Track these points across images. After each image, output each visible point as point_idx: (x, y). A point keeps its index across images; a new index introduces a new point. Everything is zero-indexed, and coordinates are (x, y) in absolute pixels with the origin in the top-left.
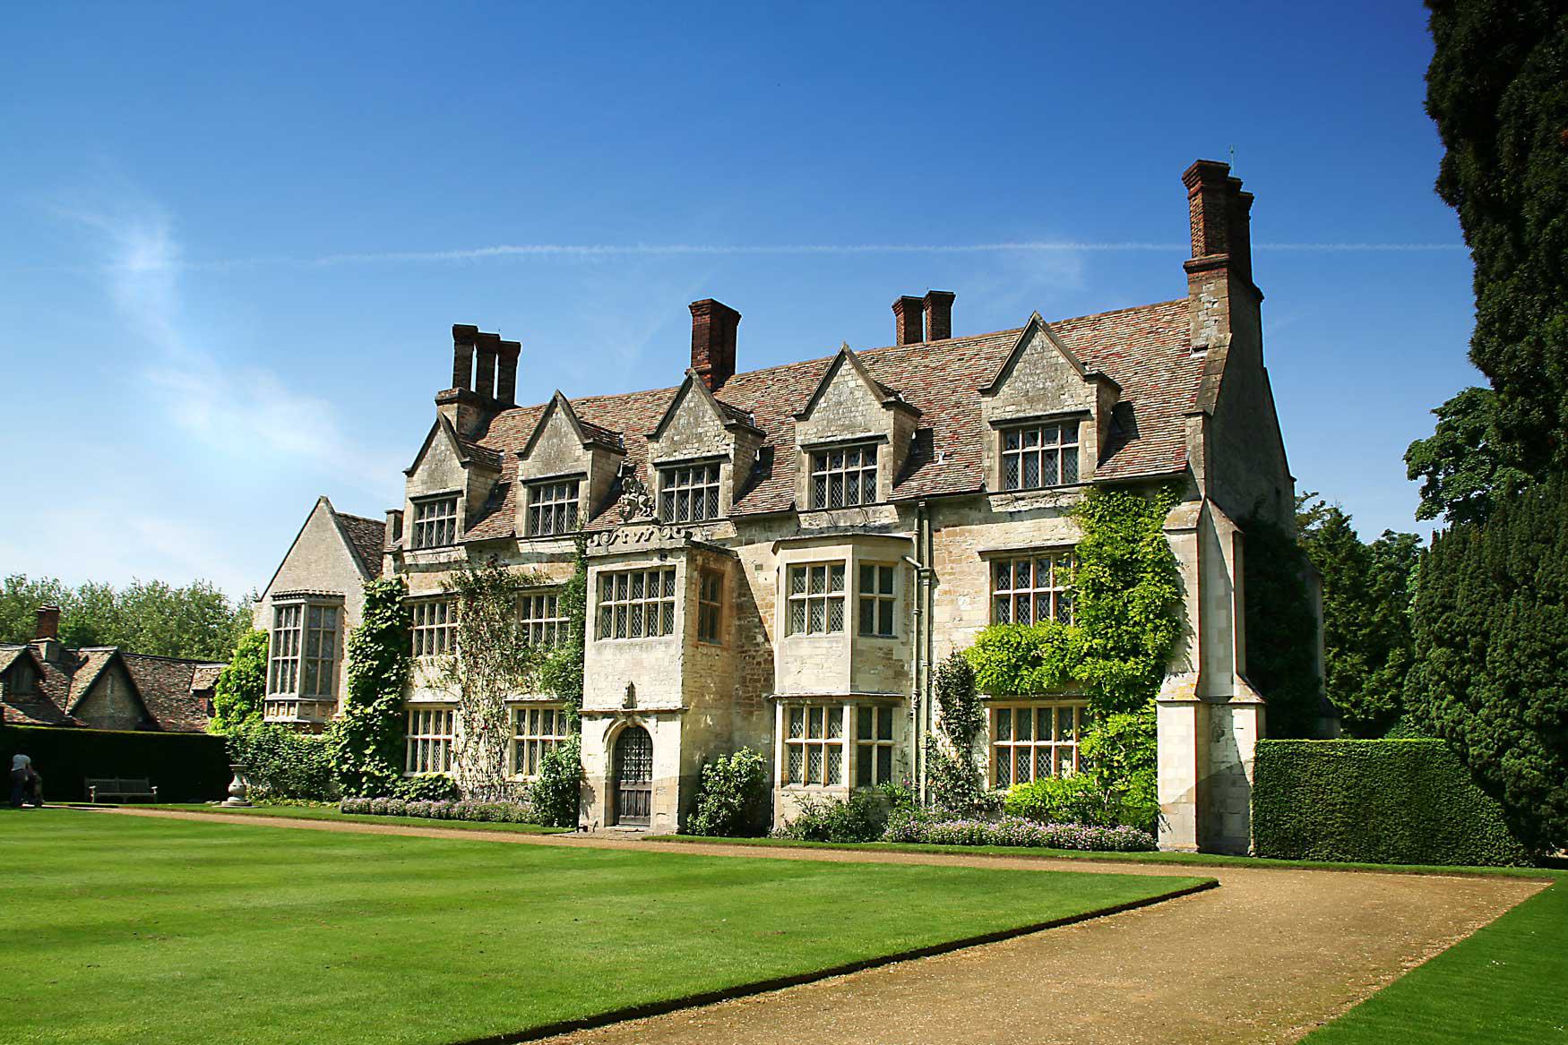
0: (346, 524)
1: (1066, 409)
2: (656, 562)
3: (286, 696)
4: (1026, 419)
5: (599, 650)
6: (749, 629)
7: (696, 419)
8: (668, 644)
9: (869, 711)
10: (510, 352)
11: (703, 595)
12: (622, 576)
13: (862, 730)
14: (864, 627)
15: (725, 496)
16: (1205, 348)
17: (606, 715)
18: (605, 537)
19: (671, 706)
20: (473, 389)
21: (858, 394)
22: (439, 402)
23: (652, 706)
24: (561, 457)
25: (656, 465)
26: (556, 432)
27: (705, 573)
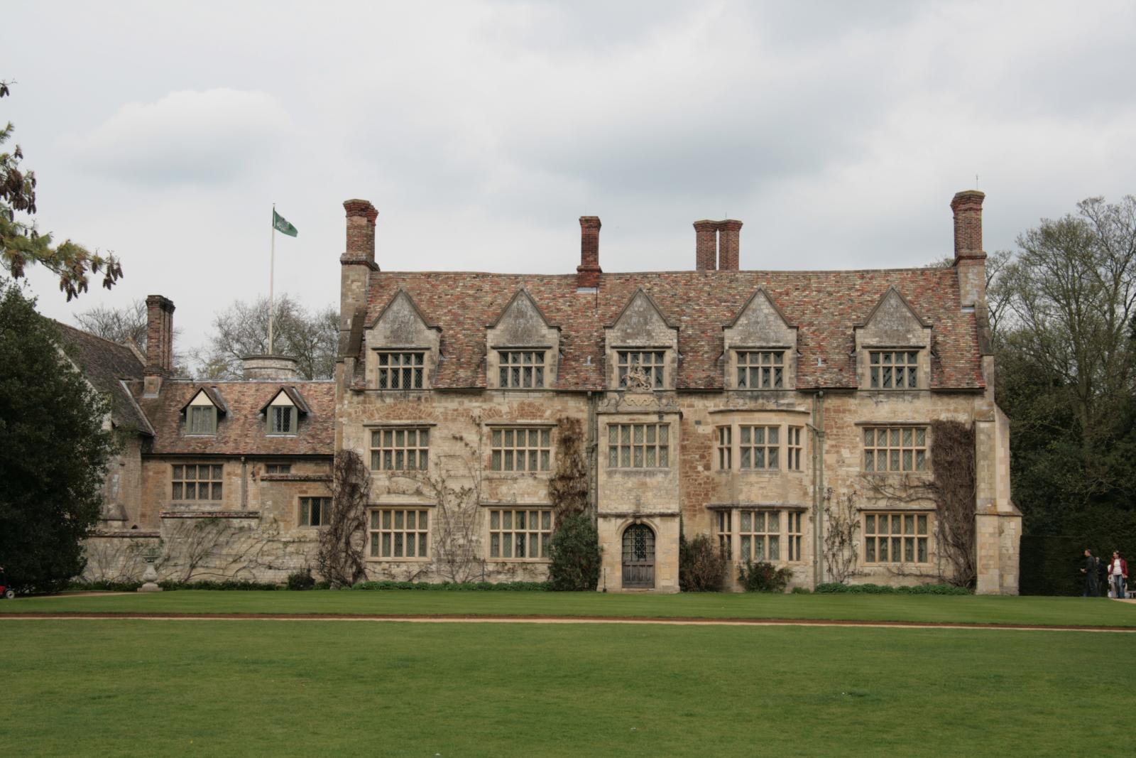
1: (911, 344)
2: (654, 418)
4: (886, 347)
5: (610, 474)
6: (692, 462)
7: (645, 320)
8: (666, 473)
12: (625, 427)
15: (670, 374)
16: (973, 306)
17: (619, 516)
19: (670, 511)
22: (344, 263)
23: (657, 511)
24: (527, 332)
25: (613, 347)
26: (521, 314)
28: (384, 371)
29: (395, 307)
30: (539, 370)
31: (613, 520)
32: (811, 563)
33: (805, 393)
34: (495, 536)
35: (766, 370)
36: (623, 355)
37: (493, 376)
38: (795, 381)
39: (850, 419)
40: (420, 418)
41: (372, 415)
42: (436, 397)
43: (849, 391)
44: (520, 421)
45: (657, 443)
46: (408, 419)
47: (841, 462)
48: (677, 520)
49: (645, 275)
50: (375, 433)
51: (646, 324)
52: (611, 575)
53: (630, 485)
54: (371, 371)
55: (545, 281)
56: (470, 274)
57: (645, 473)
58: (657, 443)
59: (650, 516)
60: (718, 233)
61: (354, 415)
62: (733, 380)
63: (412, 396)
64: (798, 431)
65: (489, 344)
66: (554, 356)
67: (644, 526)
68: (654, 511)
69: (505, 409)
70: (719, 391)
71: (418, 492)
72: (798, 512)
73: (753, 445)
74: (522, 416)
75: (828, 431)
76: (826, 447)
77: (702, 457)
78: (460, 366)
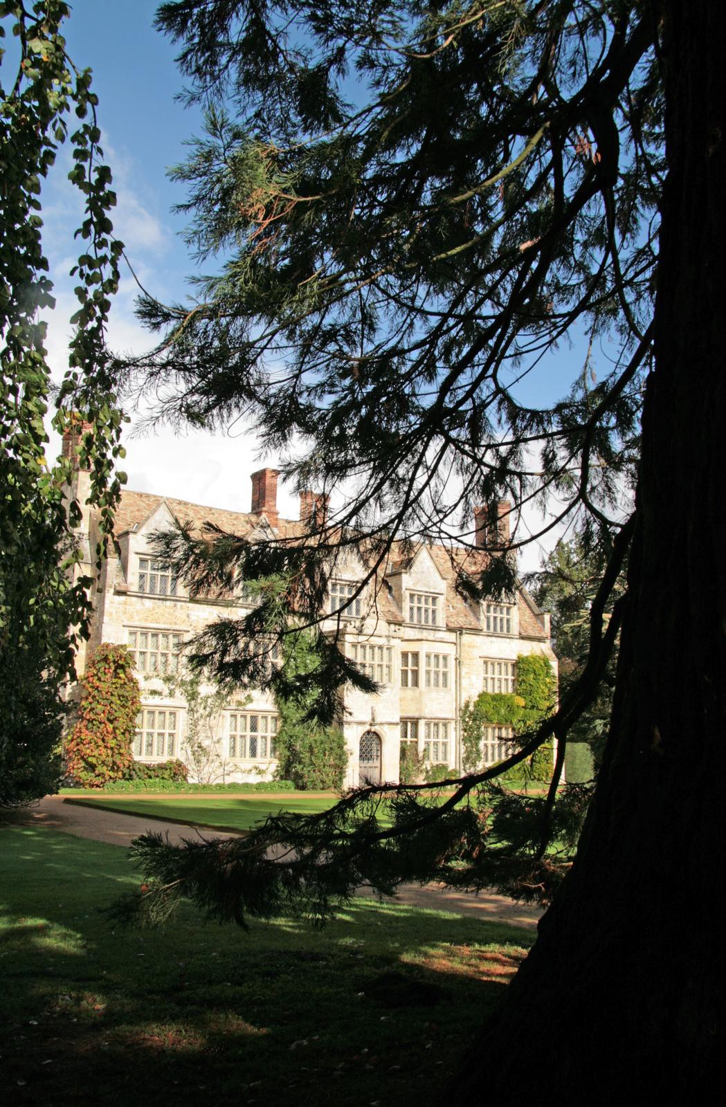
2: (382, 641)
28: (142, 576)
31: (355, 726)
33: (450, 630)
34: (233, 738)
35: (426, 611)
38: (445, 621)
40: (176, 624)
41: (132, 617)
42: (191, 605)
43: (476, 631)
45: (385, 663)
46: (165, 623)
50: (131, 633)
54: (133, 574)
55: (234, 516)
56: (174, 500)
58: (385, 663)
59: (381, 724)
61: (114, 614)
62: (406, 615)
67: (375, 733)
68: (384, 720)
70: (400, 624)
76: (463, 674)
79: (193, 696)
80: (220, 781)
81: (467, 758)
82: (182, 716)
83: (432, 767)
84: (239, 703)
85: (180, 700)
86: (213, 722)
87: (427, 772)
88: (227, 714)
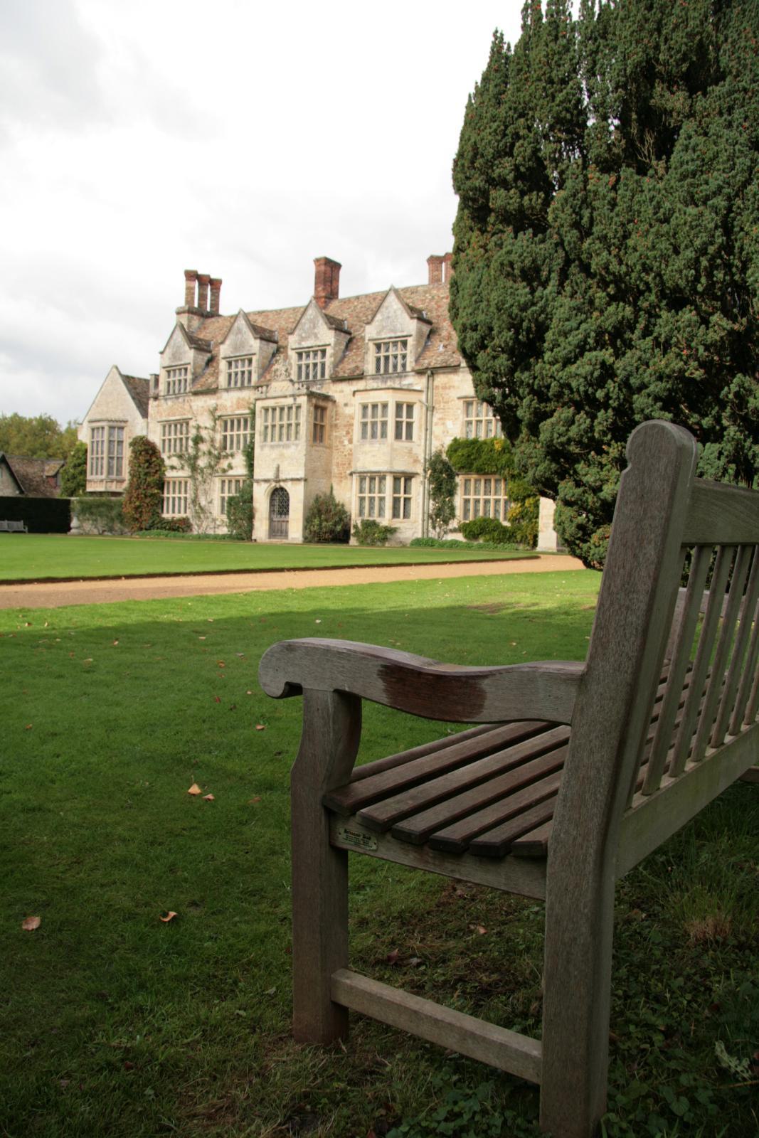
0: (129, 380)
2: (290, 401)
3: (100, 477)
5: (262, 447)
8: (297, 445)
9: (399, 479)
10: (215, 284)
11: (316, 419)
12: (274, 409)
13: (396, 490)
14: (398, 436)
17: (266, 481)
18: (264, 388)
19: (298, 477)
20: (196, 305)
21: (399, 312)
24: (242, 345)
26: (239, 331)
27: (316, 407)
29: (174, 337)
30: (250, 373)
32: (420, 522)
33: (420, 373)
36: (300, 355)
37: (223, 381)
38: (414, 364)
39: (454, 394)
42: (192, 398)
44: (237, 412)
45: (293, 421)
47: (446, 432)
48: (302, 483)
49: (358, 298)
51: (314, 328)
52: (261, 529)
53: (274, 456)
57: (283, 446)
59: (285, 480)
60: (444, 265)
62: (370, 368)
63: (181, 400)
64: (410, 407)
65: (222, 355)
66: (258, 361)
67: (282, 489)
69: (229, 404)
70: (361, 377)
71: (182, 468)
72: (409, 477)
73: (369, 420)
74: (238, 408)
75: (437, 406)
76: (435, 420)
77: (348, 433)
78: (212, 375)
79: (194, 468)
80: (211, 532)
81: (438, 515)
82: (190, 482)
83: (362, 521)
84: (224, 471)
85: (186, 472)
86: (207, 487)
87: (356, 527)
88: (217, 482)
